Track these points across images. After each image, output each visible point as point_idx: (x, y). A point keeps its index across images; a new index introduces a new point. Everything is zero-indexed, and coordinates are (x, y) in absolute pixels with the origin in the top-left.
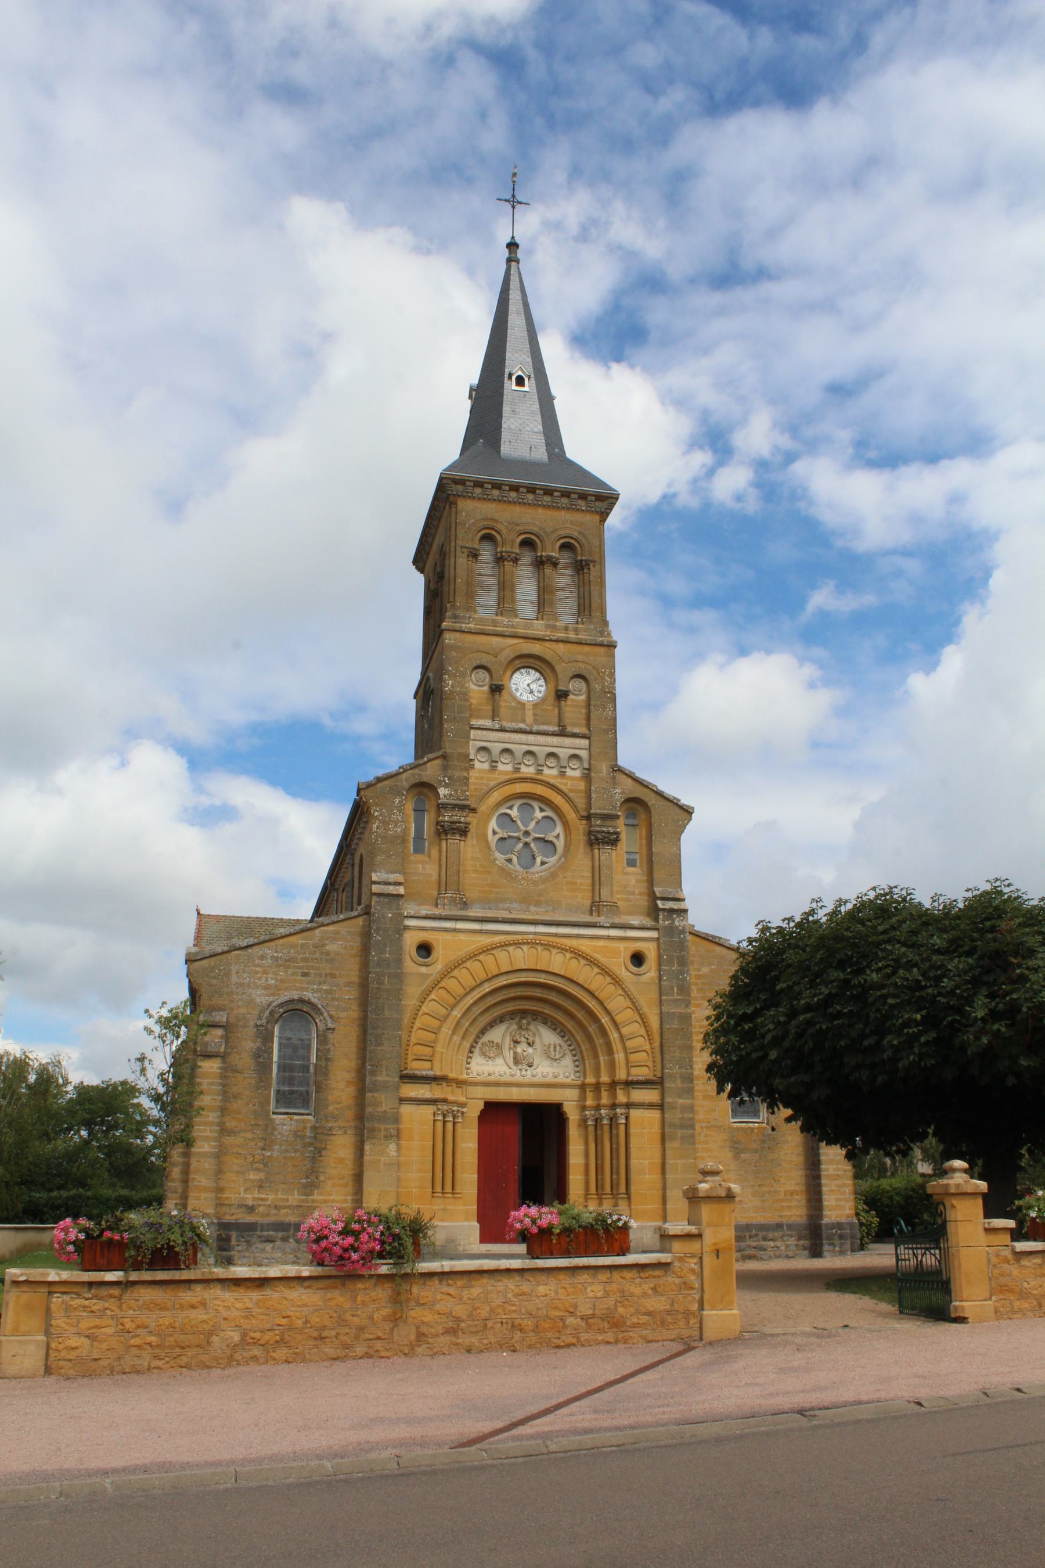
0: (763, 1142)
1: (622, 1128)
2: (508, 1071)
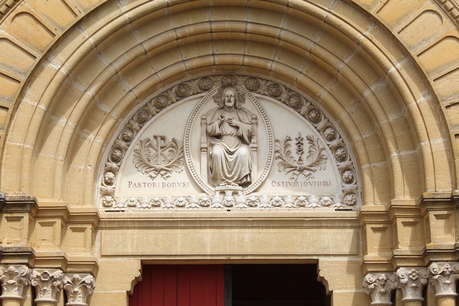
2: (196, 196)
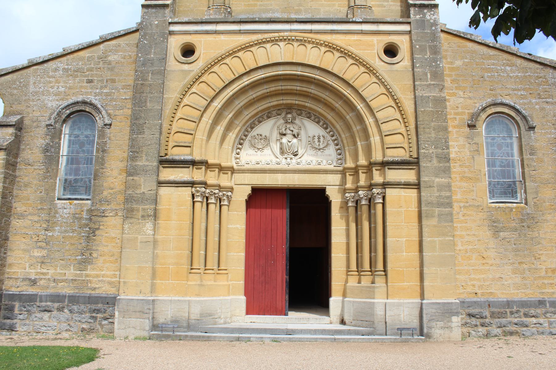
0: (522, 221)
1: (380, 207)
2: (274, 160)
